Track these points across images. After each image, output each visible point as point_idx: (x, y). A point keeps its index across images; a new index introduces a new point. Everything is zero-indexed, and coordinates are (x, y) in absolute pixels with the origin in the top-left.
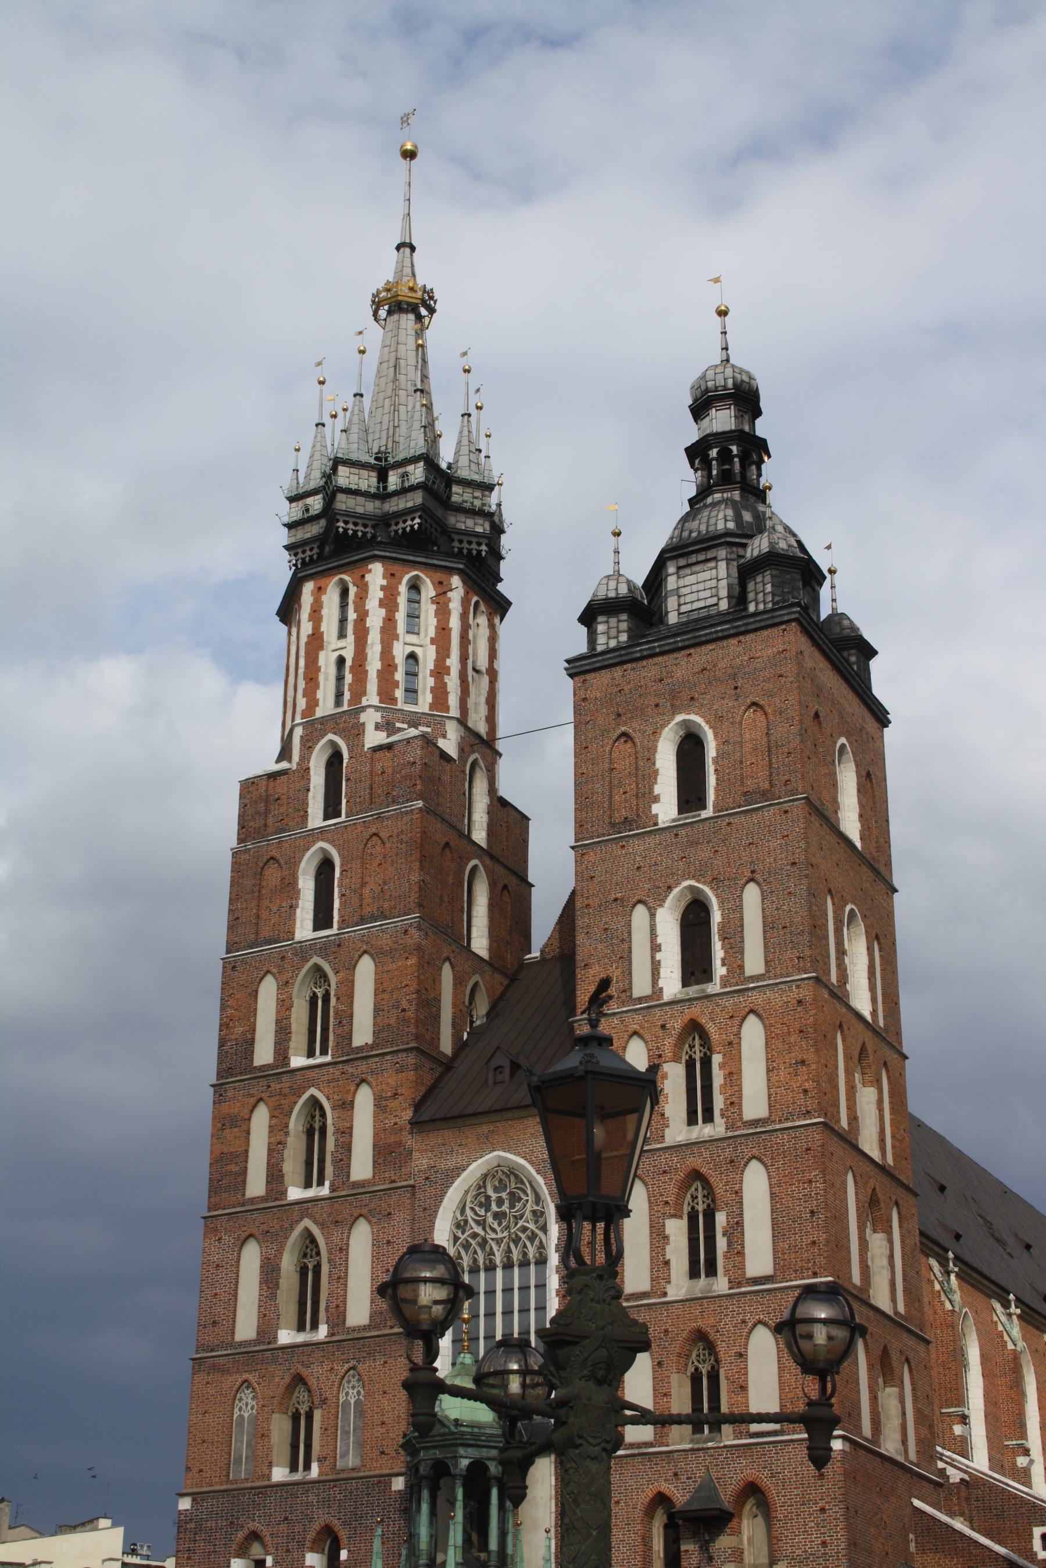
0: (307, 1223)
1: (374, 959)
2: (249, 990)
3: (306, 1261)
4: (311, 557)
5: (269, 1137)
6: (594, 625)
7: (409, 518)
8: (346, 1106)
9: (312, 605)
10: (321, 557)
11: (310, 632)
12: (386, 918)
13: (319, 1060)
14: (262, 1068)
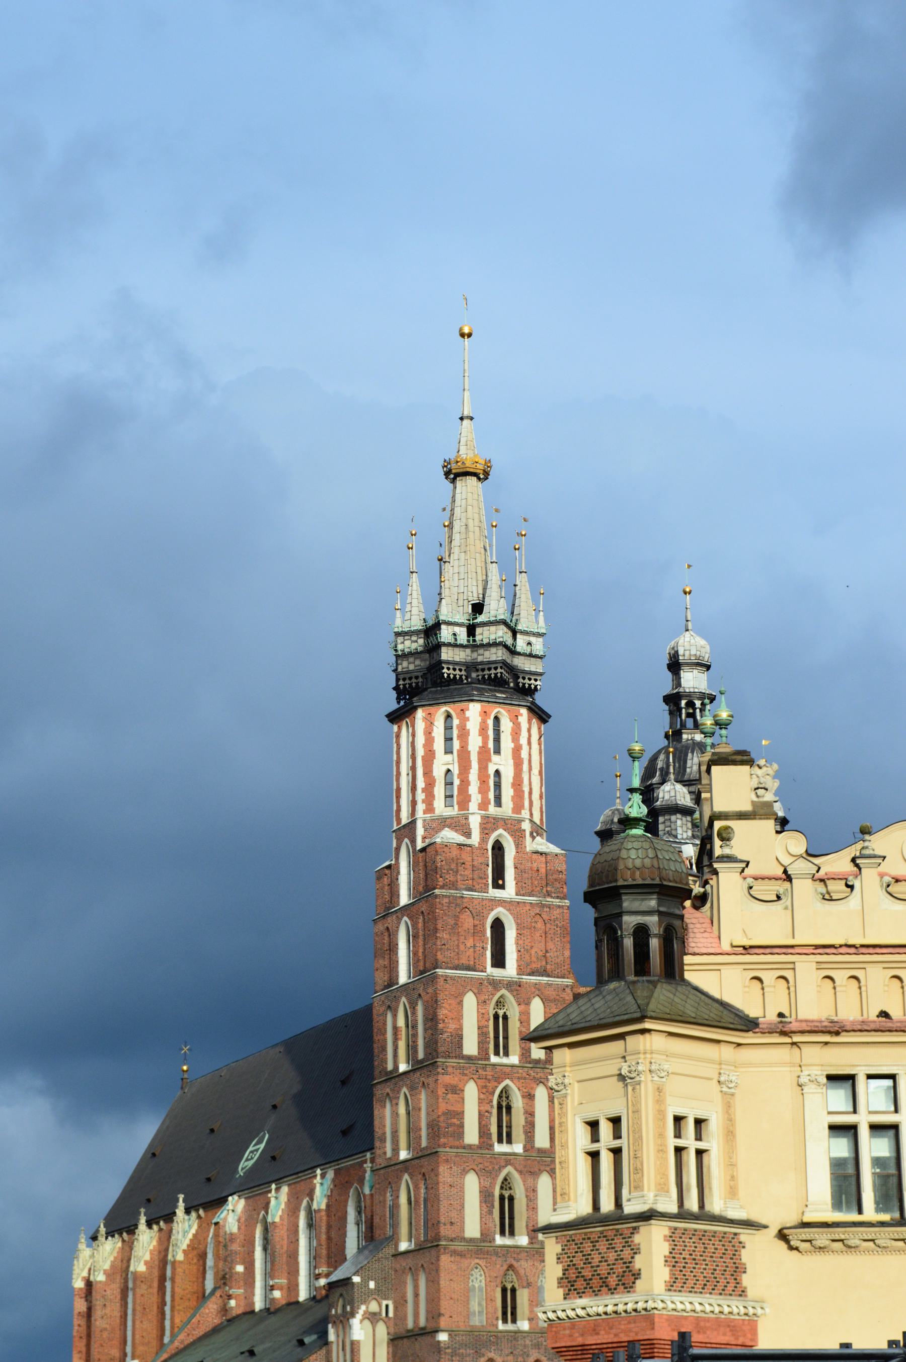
0: (509, 1169)
1: (544, 1004)
2: (458, 1000)
3: (504, 1192)
4: (461, 676)
5: (479, 1106)
6: (673, 818)
7: (533, 678)
8: (530, 1097)
9: (480, 723)
10: (467, 678)
11: (481, 745)
12: (548, 976)
13: (505, 1060)
14: (469, 1058)
